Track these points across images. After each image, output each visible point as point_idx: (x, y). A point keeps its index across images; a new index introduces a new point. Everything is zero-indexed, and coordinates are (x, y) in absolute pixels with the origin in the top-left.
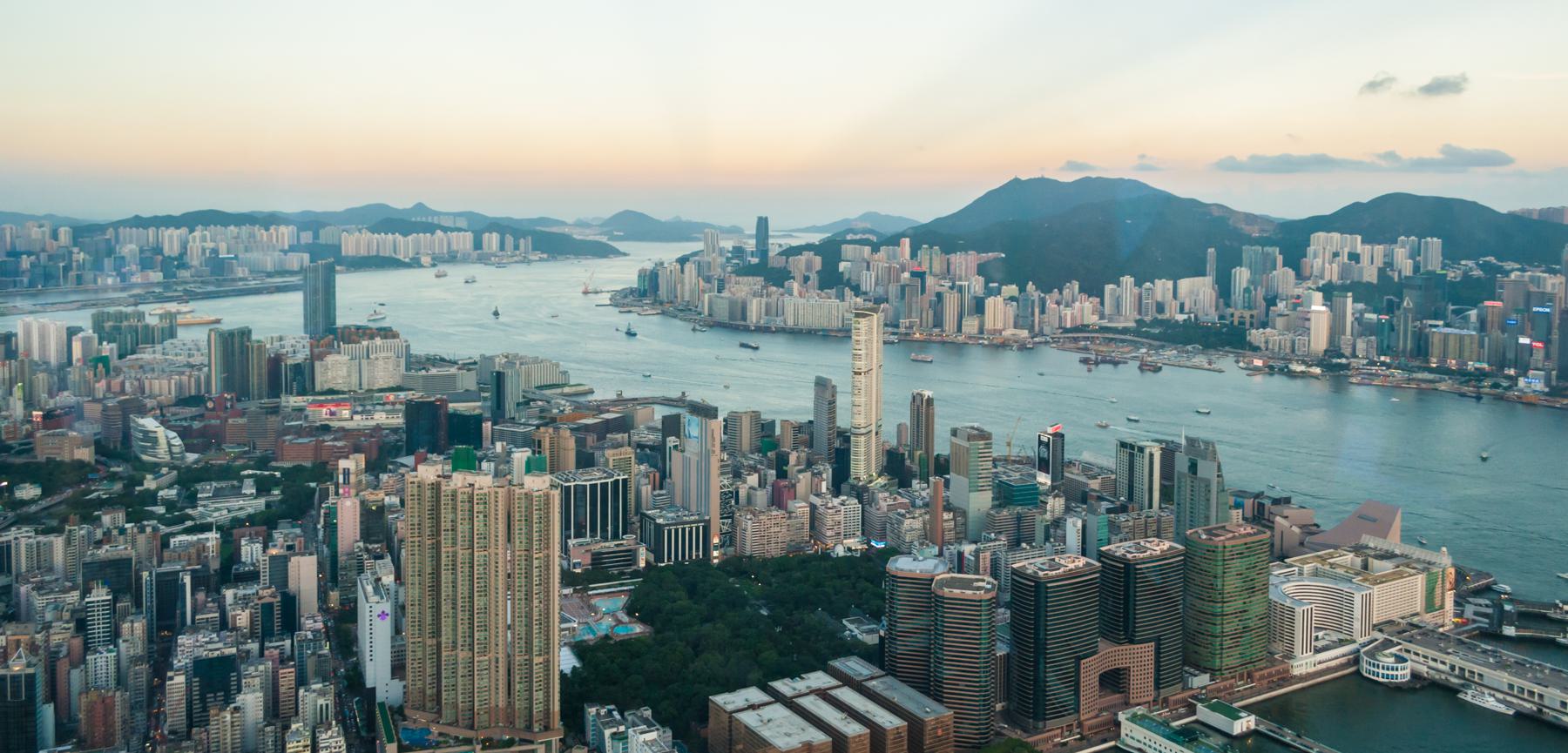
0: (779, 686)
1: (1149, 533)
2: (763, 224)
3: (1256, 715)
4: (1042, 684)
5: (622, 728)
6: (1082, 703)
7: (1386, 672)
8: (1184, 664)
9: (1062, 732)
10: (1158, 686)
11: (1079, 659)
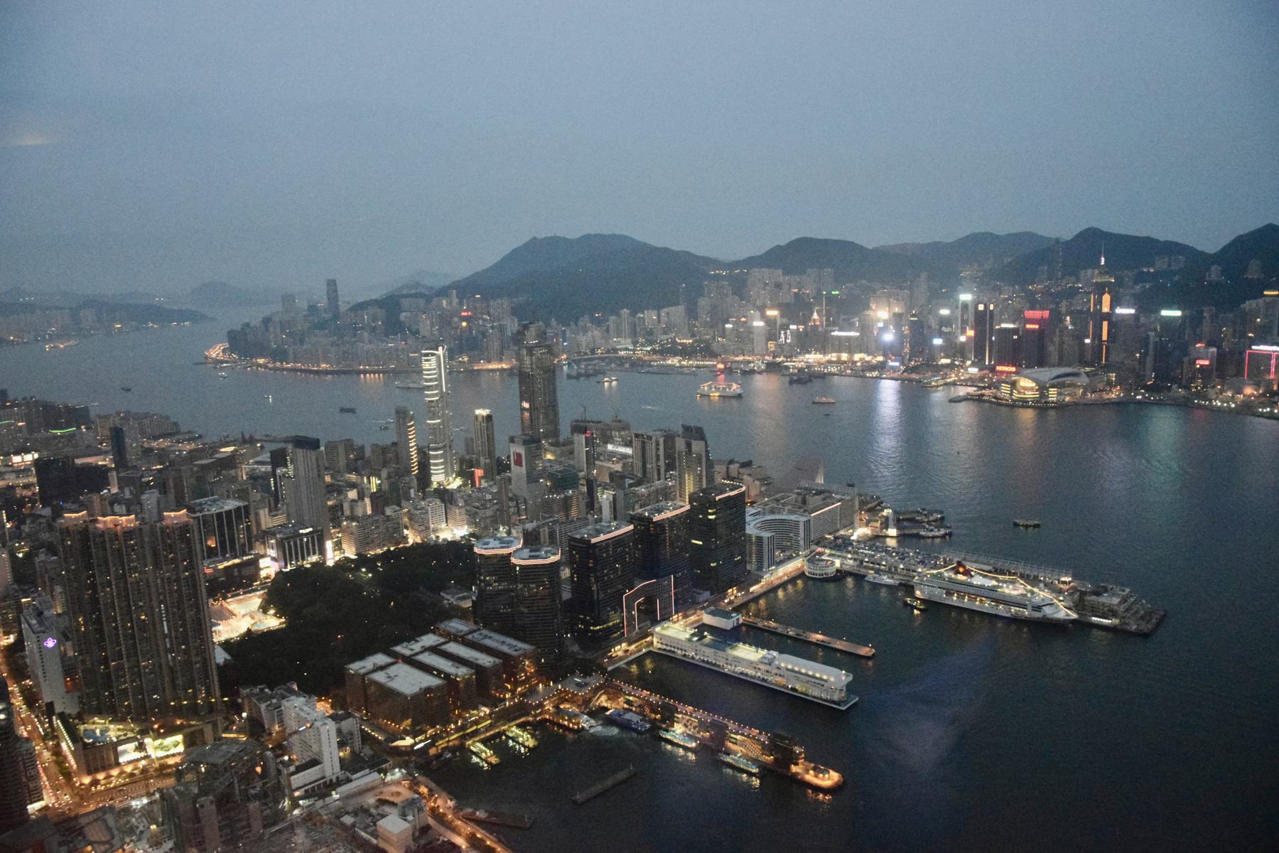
0: (398, 649)
2: (332, 284)
5: (274, 701)
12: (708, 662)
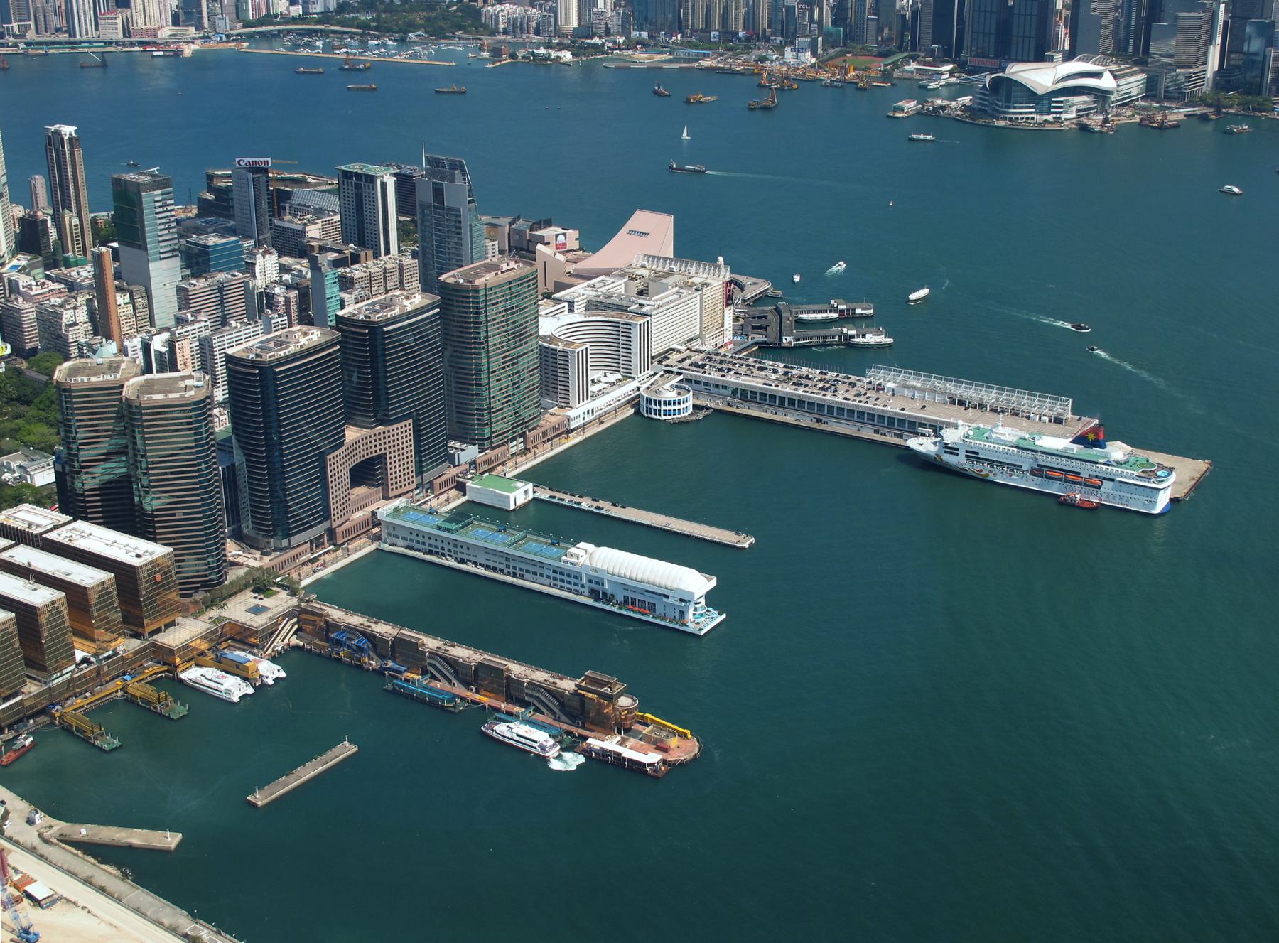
1: (390, 284)
4: (281, 493)
7: (668, 408)
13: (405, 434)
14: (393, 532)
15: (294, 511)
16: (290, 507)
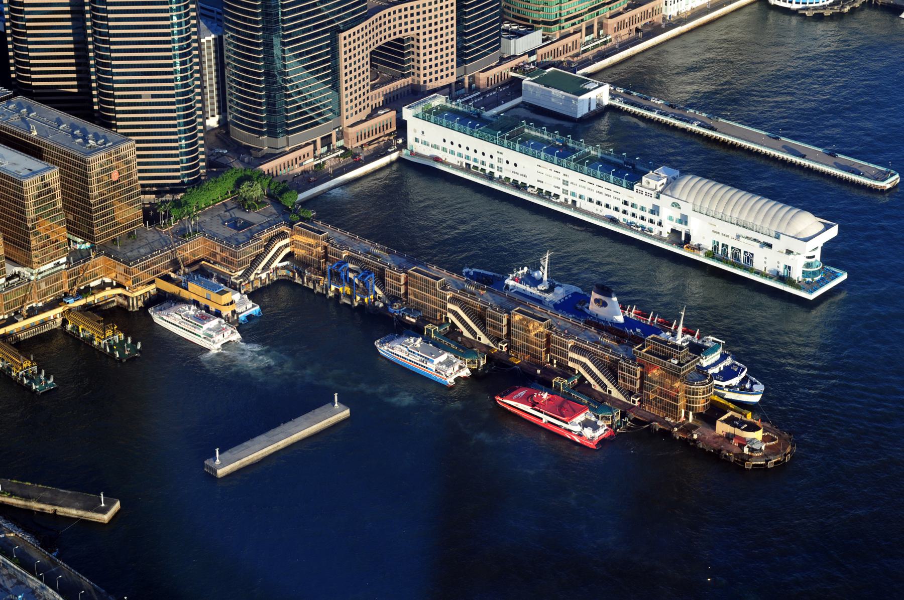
3: (612, 84)
4: (279, 79)
6: (344, 100)
8: (502, 21)
9: (315, 149)
10: (462, 58)
11: (338, 30)
12: (522, 187)
13: (445, 10)
14: (421, 138)
15: (295, 102)
16: (290, 96)
